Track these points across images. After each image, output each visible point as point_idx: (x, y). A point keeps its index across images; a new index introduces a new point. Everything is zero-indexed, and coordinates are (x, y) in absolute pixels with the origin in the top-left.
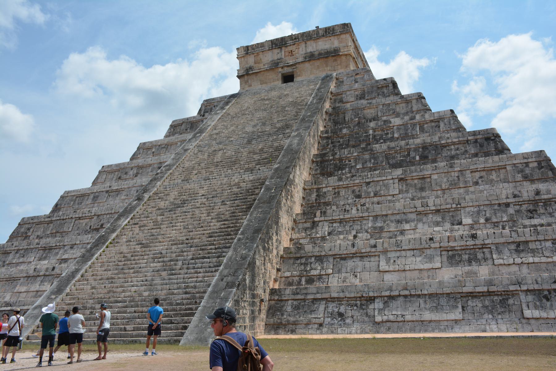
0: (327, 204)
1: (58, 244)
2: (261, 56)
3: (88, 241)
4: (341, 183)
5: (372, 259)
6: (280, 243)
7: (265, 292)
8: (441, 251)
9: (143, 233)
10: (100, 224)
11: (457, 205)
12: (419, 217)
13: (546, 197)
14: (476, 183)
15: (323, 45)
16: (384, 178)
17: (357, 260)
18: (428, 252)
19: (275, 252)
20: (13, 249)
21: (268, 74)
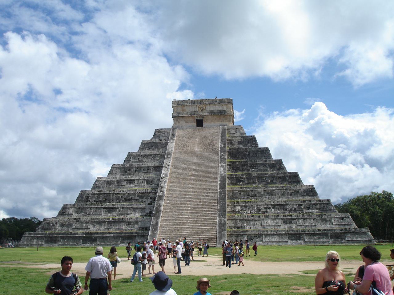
0: (237, 198)
1: (114, 206)
2: (185, 107)
3: (131, 206)
4: (242, 190)
5: (259, 221)
9: (175, 208)
10: (130, 198)
13: (312, 203)
14: (291, 195)
15: (218, 108)
16: (258, 189)
17: (254, 221)
18: (277, 220)
20: (88, 207)
21: (189, 118)
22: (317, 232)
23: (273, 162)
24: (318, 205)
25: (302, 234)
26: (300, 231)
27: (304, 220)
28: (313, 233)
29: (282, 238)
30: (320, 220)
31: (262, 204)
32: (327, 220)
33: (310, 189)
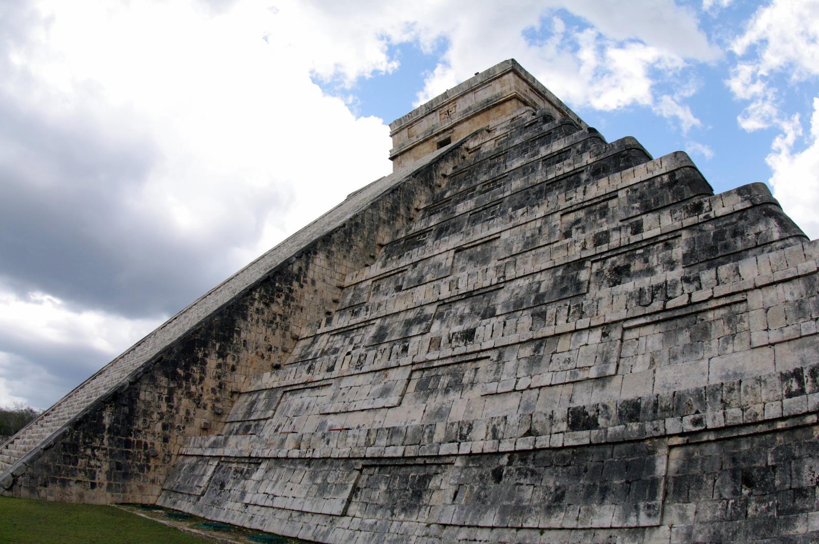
5: (323, 392)
6: (233, 369)
7: (166, 440)
8: (412, 371)
11: (499, 279)
12: (441, 309)
13: (646, 235)
16: (436, 252)
18: (393, 374)
19: (210, 382)
22: (558, 441)
23: (561, 147)
24: (685, 235)
25: (440, 462)
26: (439, 435)
27: (536, 350)
28: (523, 445)
29: (323, 489)
30: (649, 330)
31: (403, 308)
32: (710, 316)
33: (666, 178)
